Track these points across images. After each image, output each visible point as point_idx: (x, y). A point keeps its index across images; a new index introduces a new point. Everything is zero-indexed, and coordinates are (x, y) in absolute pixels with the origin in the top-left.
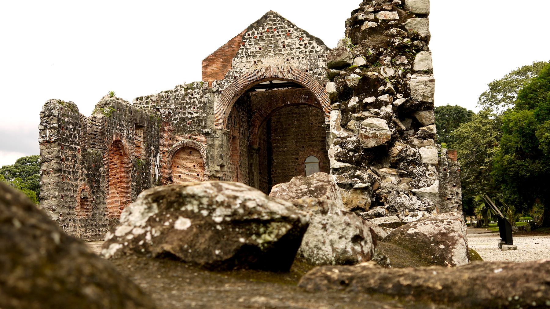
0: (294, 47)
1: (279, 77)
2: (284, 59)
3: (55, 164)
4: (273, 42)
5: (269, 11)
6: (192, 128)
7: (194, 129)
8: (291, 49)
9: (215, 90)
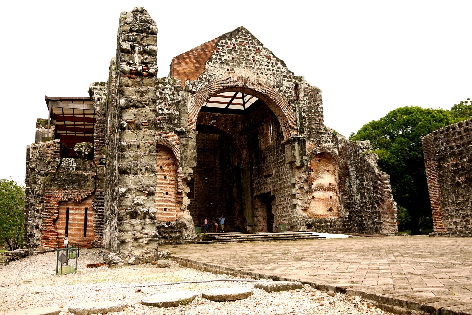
0: (263, 63)
3: (151, 113)
4: (244, 54)
5: (240, 26)
6: (163, 125)
8: (260, 65)
9: (190, 89)
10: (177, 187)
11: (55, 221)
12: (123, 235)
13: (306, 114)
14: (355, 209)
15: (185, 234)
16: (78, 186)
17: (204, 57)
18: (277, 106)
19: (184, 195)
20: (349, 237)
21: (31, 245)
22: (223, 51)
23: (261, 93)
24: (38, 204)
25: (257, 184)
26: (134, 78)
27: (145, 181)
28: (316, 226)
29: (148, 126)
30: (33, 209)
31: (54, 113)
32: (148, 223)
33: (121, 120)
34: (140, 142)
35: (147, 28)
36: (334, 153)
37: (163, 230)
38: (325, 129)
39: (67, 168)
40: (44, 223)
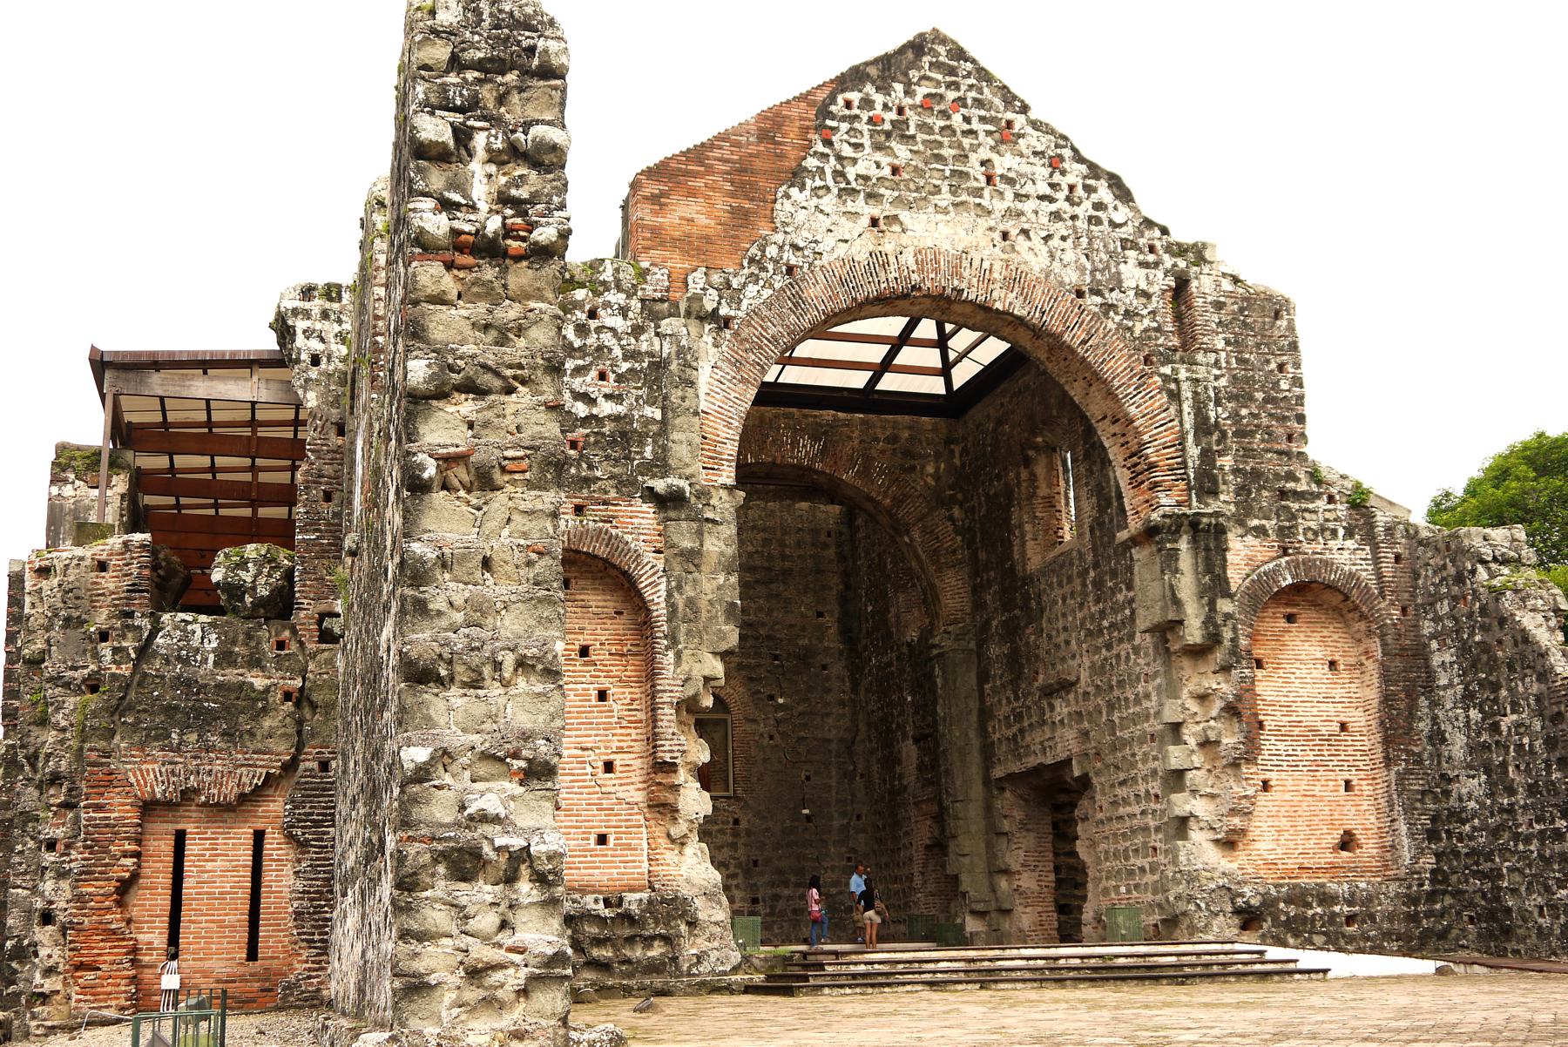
0: (1029, 189)
1: (972, 297)
2: (990, 229)
3: (542, 416)
4: (947, 152)
5: (927, 29)
6: (591, 467)
7: (598, 474)
8: (1017, 196)
9: (709, 306)
10: (653, 739)
11: (125, 887)
12: (416, 955)
13: (1225, 409)
14: (1460, 840)
15: (690, 949)
16: (223, 735)
17: (767, 166)
18: (1094, 378)
19: (682, 776)
20: (1439, 971)
21: (21, 993)
22: (853, 140)
23: (1020, 319)
24: (55, 813)
25: (1009, 726)
26: (469, 268)
27: (514, 714)
28: (1283, 918)
29: (527, 475)
30: (33, 838)
31: (128, 417)
32: (525, 901)
33: (413, 447)
34: (493, 542)
35: (524, 50)
36: (1357, 585)
37: (592, 930)
38: (1315, 476)
39: (179, 658)
40: (79, 899)
